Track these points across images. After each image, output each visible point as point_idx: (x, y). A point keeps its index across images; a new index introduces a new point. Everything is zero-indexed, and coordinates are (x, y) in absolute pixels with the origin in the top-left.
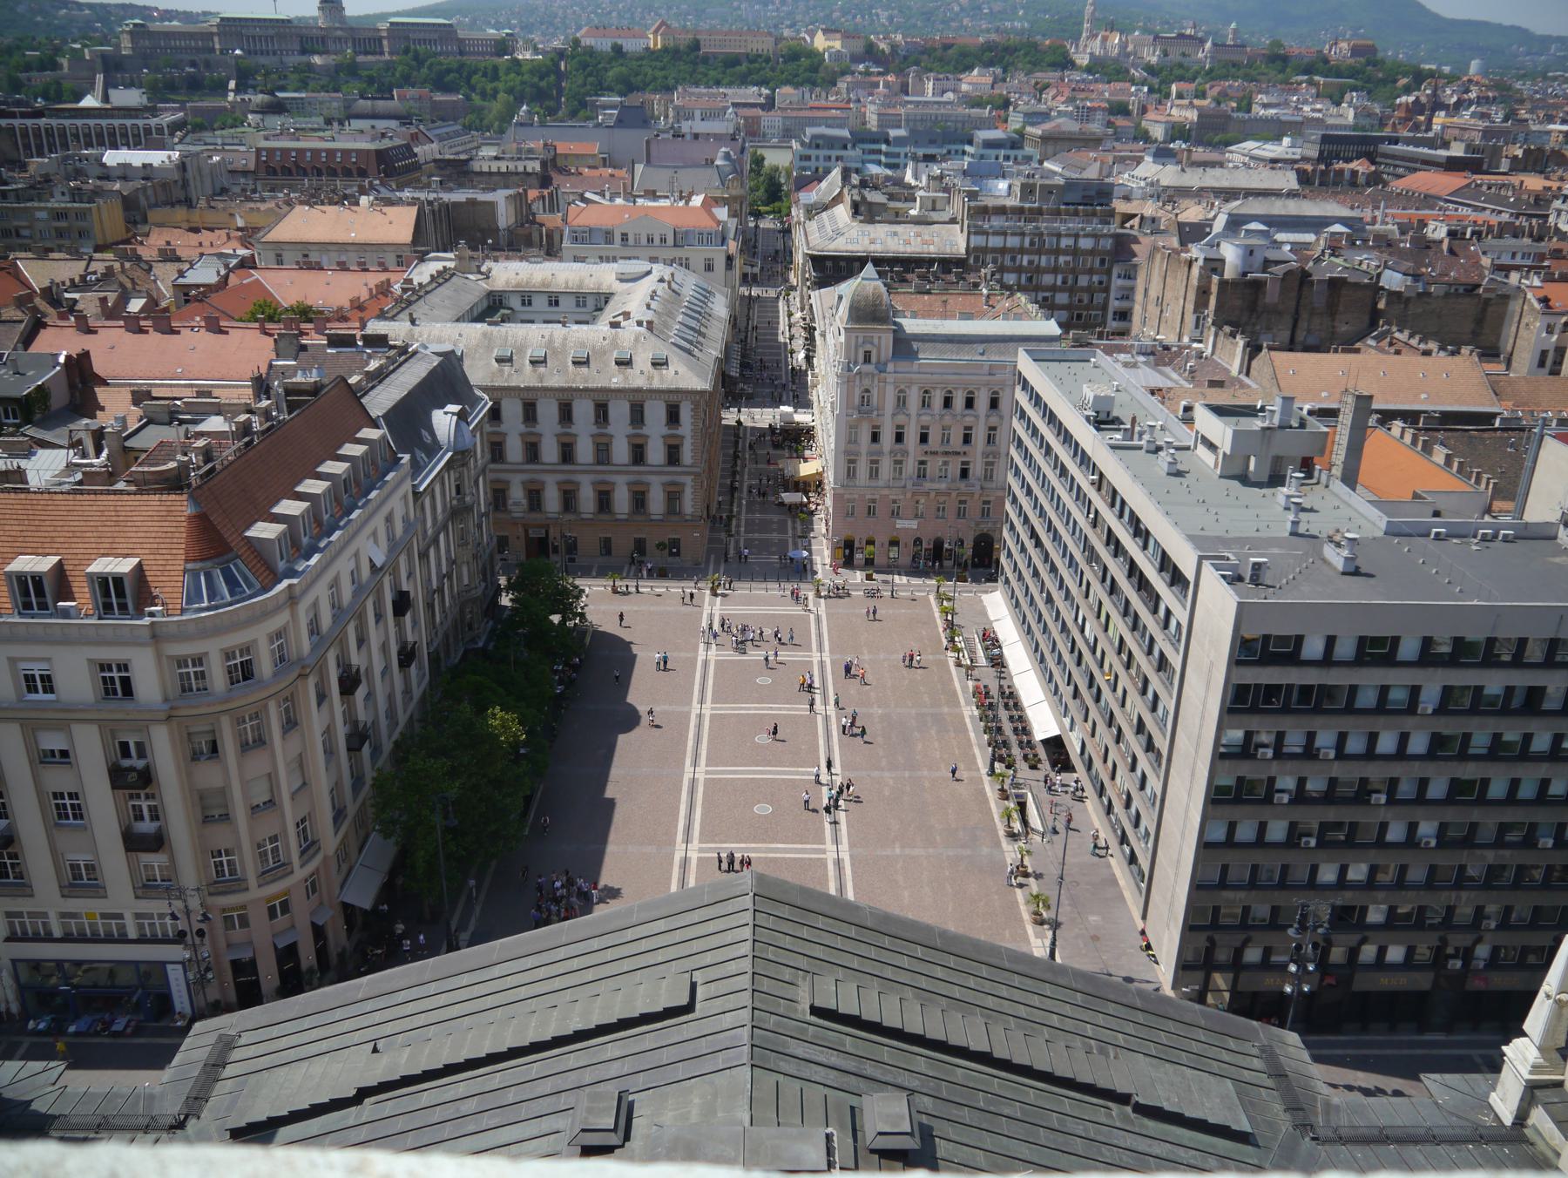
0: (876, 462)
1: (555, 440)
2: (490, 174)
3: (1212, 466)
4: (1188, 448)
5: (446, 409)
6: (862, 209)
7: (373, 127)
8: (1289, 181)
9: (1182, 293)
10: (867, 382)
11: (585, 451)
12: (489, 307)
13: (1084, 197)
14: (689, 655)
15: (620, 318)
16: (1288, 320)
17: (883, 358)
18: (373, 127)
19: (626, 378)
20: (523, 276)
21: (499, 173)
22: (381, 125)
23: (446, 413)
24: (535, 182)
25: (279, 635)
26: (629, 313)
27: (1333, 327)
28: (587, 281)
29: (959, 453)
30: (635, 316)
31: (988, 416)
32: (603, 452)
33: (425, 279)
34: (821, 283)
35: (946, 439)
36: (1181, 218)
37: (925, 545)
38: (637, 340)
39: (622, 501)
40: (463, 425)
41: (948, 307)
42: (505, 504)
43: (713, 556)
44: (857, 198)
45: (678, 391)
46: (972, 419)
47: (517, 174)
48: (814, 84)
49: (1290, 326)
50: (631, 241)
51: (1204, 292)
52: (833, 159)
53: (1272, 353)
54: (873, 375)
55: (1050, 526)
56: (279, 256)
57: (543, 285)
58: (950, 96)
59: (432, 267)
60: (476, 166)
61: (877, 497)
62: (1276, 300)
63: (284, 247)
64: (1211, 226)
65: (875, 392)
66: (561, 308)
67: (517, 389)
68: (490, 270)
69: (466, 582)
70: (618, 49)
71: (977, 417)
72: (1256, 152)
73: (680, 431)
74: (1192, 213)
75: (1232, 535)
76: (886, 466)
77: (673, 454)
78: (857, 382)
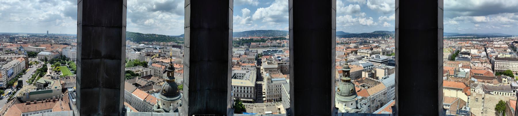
35: (276, 90)
48: (264, 42)
70: (246, 39)
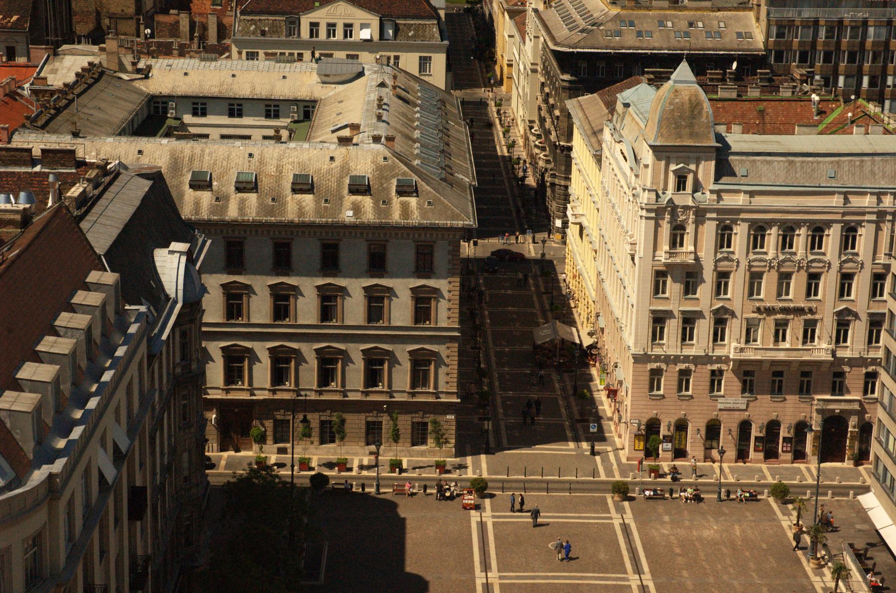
15: (346, 133)
25: (37, 540)
33: (71, 78)
34: (575, 90)
41: (767, 119)
46: (821, 265)
65: (690, 228)
68: (149, 68)
69: (186, 473)
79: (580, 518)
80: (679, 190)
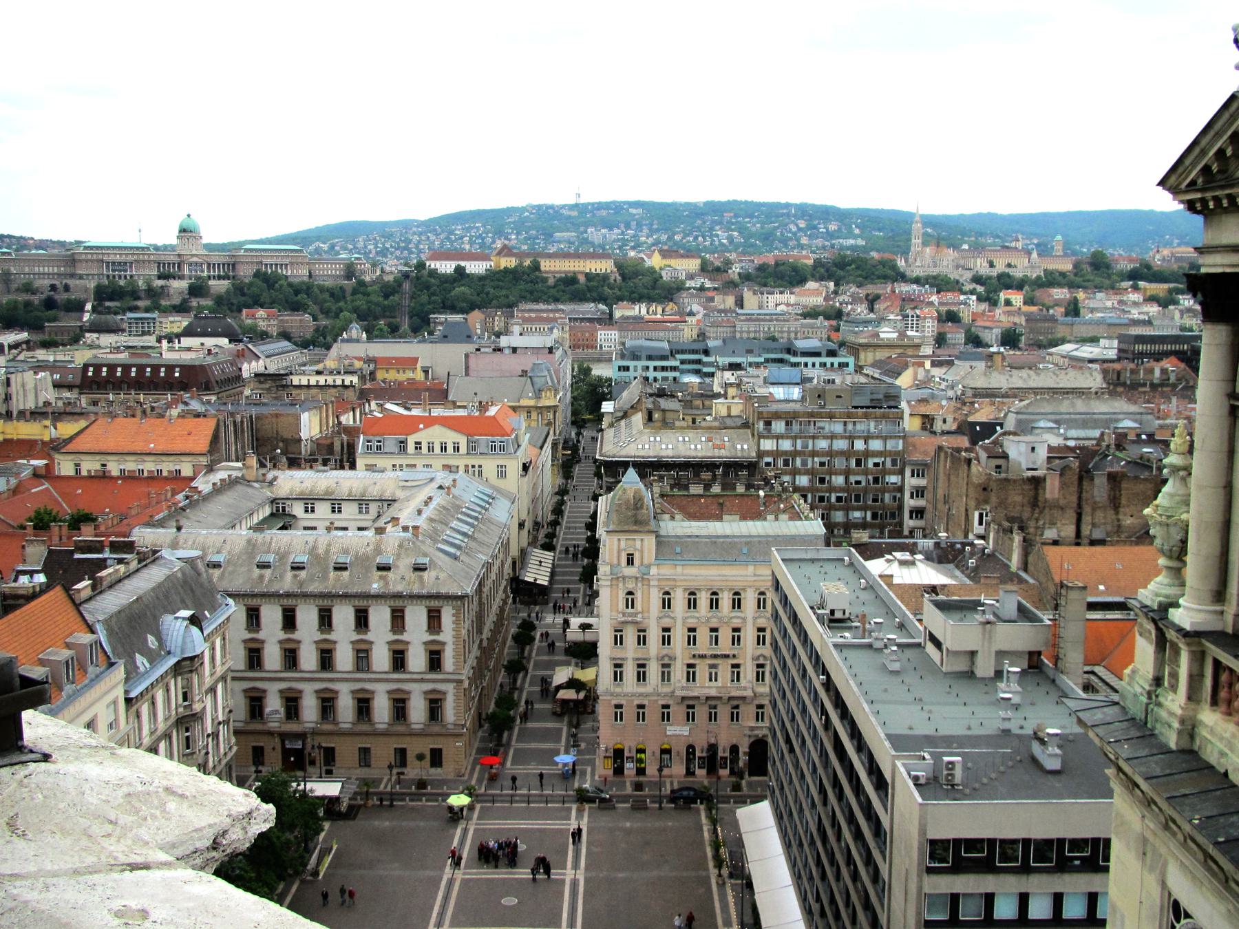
0: (643, 666)
1: (314, 647)
2: (308, 386)
3: (939, 663)
4: (918, 645)
5: (176, 615)
6: (656, 416)
7: (202, 344)
8: (1095, 380)
9: (965, 491)
10: (630, 586)
11: (344, 658)
12: (272, 515)
13: (872, 400)
14: (432, 873)
16: (1071, 515)
17: (646, 562)
18: (202, 344)
19: (387, 584)
20: (307, 485)
21: (317, 386)
22: (210, 342)
23: (177, 618)
24: (350, 395)
26: (397, 519)
27: (1119, 520)
28: (370, 489)
29: (727, 656)
30: (403, 522)
31: (755, 619)
32: (362, 656)
36: (971, 419)
37: (698, 754)
38: (401, 546)
39: (382, 709)
40: (195, 630)
42: (261, 714)
43: (478, 767)
44: (650, 406)
45: (438, 597)
47: (335, 386)
49: (1074, 521)
50: (425, 450)
51: (985, 489)
52: (651, 369)
53: (1046, 548)
54: (637, 578)
55: (799, 733)
56: (77, 465)
57: (327, 493)
58: (782, 308)
59: (219, 476)
60: (296, 380)
61: (645, 702)
62: (1057, 496)
63: (83, 457)
64: (1001, 425)
65: (638, 595)
66: (343, 515)
67: (276, 595)
68: (275, 478)
70: (460, 271)
71: (744, 619)
72: (1075, 353)
73: (440, 638)
74: (983, 413)
75: (942, 732)
76: (653, 670)
77: (435, 661)
78: (621, 585)
79: (500, 824)
80: (628, 564)
